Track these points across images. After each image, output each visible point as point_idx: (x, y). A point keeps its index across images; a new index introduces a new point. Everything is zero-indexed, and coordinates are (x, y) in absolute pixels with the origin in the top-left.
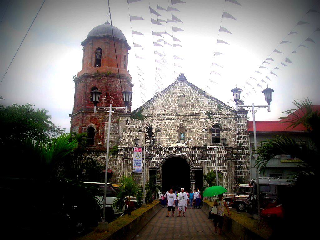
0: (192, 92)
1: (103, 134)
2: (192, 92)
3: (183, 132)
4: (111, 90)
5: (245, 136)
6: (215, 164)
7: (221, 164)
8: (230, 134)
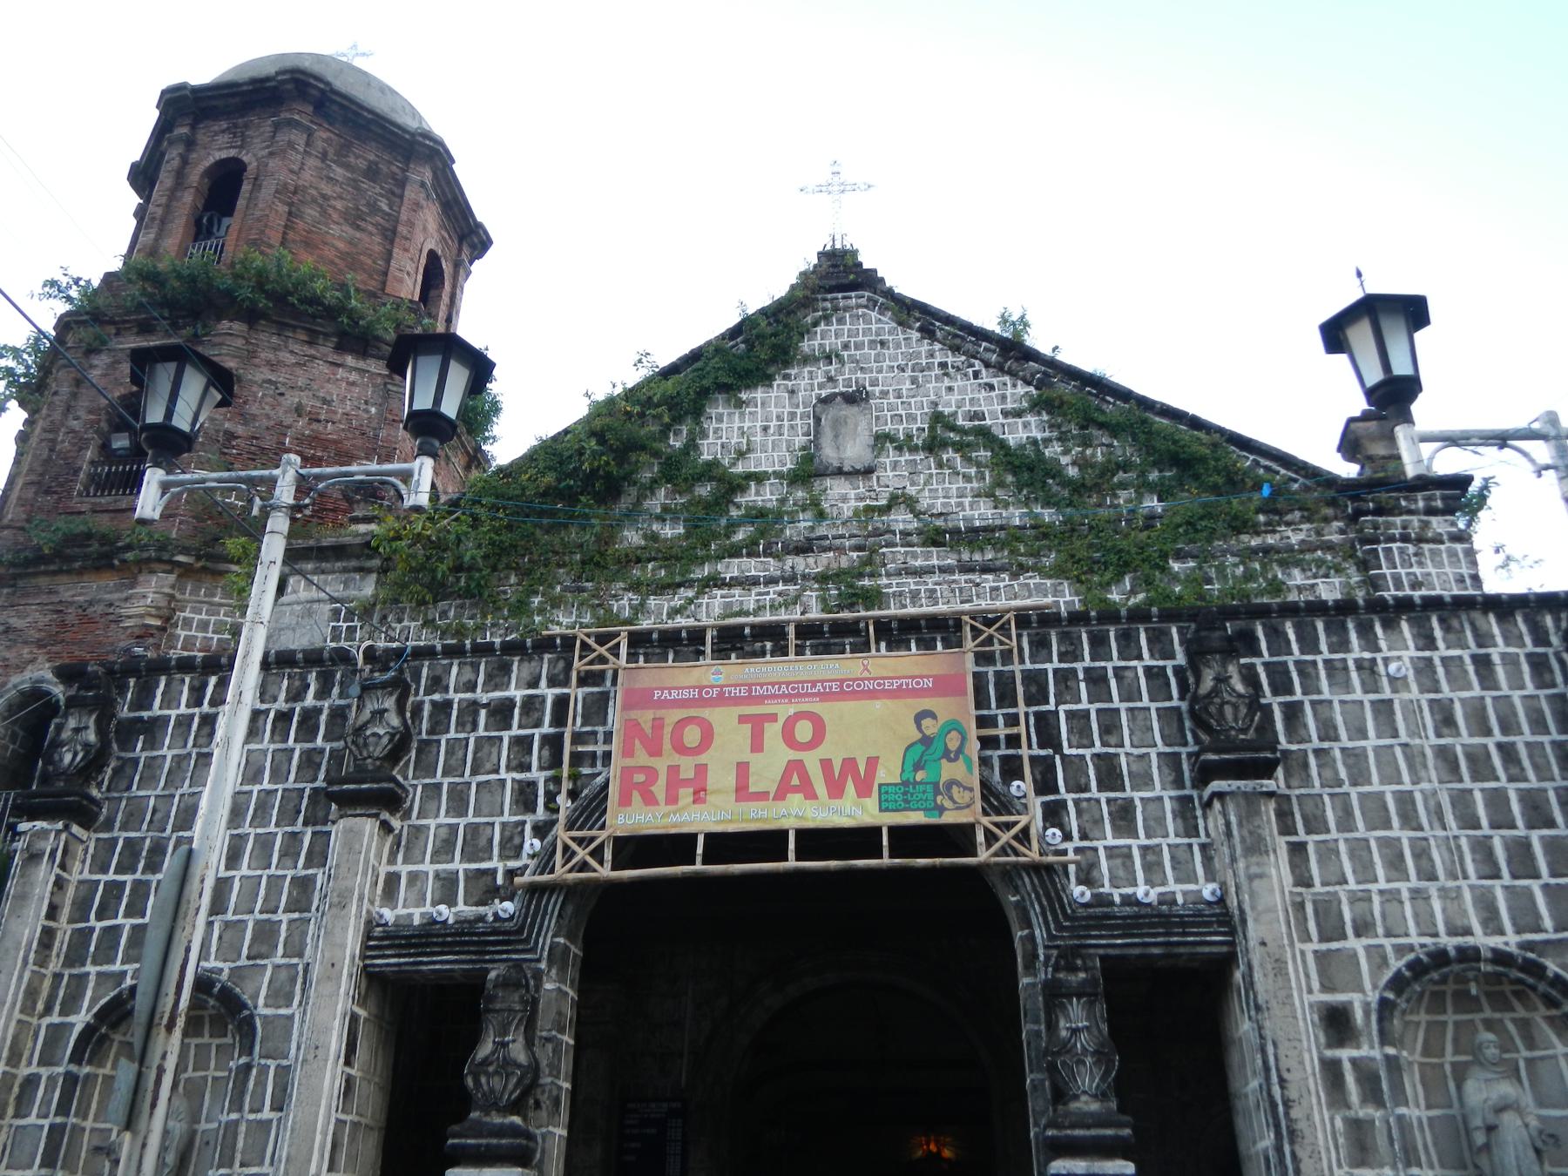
0: (929, 367)
4: (268, 417)
6: (1422, 853)
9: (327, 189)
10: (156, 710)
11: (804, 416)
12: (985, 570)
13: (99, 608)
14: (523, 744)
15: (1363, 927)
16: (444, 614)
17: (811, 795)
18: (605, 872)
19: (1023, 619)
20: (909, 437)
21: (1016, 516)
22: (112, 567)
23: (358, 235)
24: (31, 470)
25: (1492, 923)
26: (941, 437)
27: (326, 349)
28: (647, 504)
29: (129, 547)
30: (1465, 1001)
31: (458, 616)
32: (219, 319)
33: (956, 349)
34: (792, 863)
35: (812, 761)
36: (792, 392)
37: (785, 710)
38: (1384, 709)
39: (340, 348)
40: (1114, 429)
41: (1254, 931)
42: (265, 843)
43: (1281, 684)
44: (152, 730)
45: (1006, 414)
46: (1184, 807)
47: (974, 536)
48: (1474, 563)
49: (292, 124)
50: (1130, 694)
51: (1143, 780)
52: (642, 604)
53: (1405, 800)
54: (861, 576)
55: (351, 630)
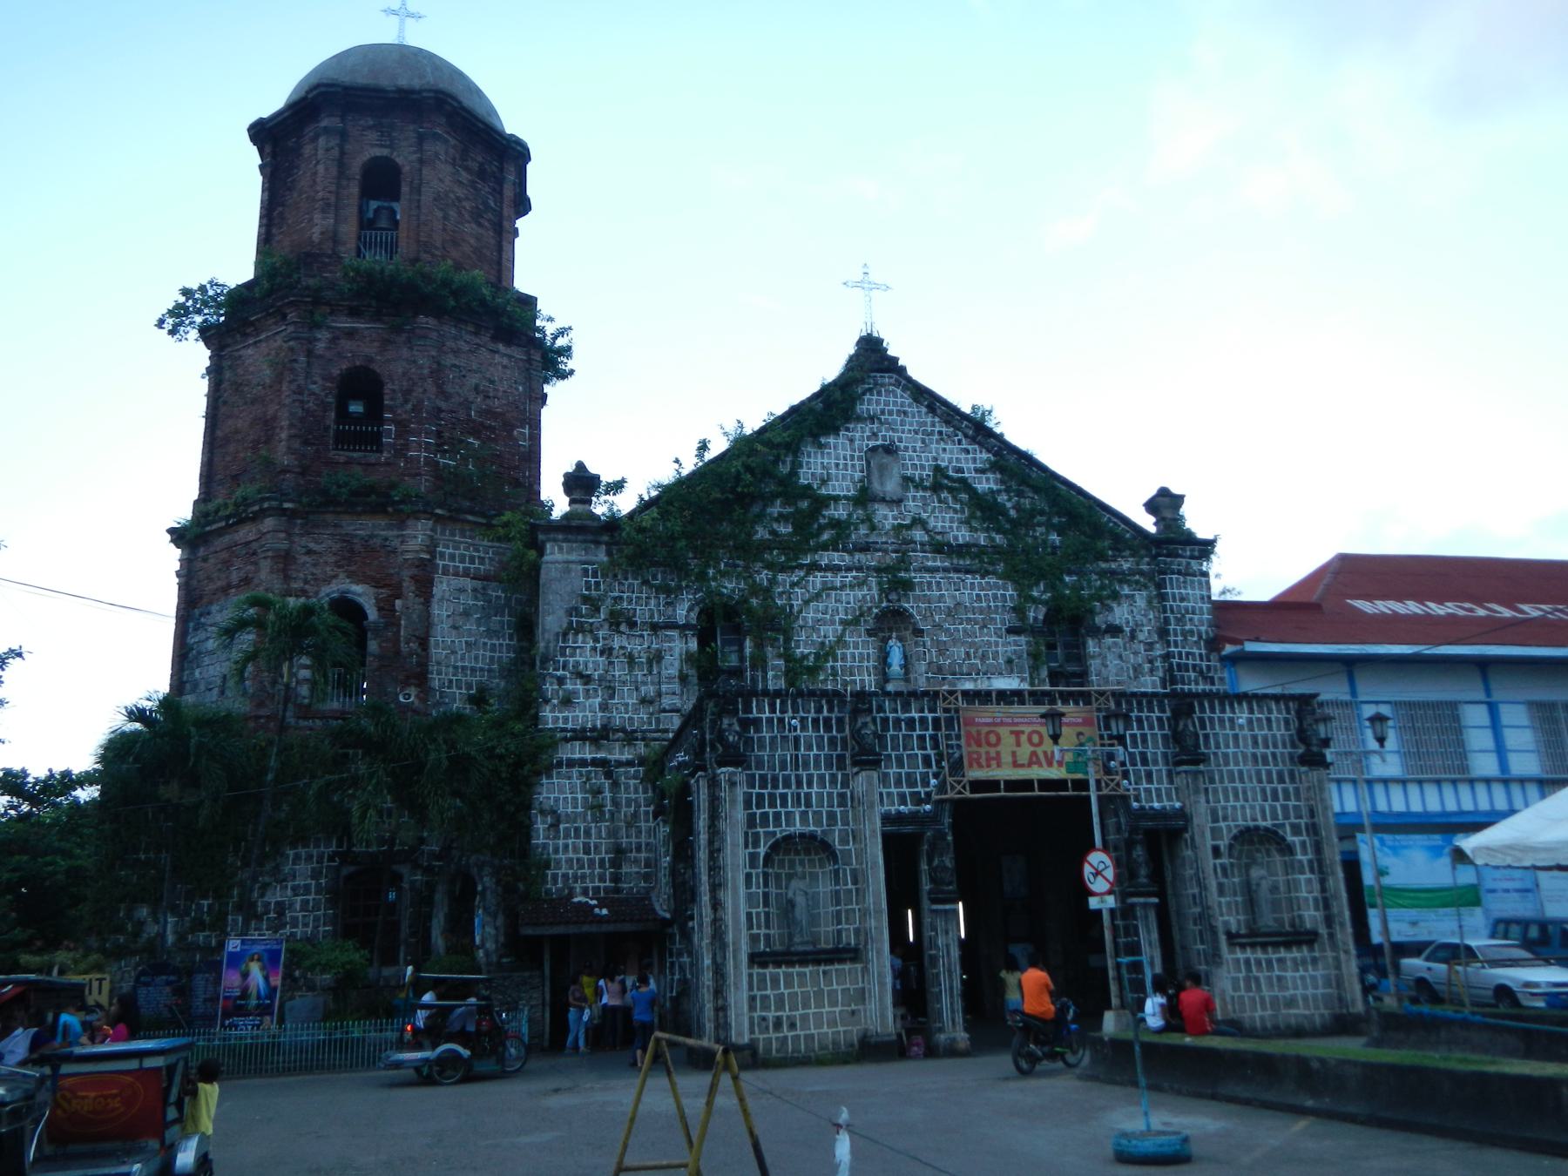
0: (932, 433)
1: (424, 643)
2: (932, 433)
3: (900, 639)
5: (1209, 667)
6: (1245, 792)
7: (1274, 792)
8: (1136, 653)
9: (460, 192)
10: (755, 714)
11: (860, 458)
12: (967, 572)
13: (378, 541)
14: (922, 738)
15: (1225, 819)
16: (655, 578)
17: (1040, 765)
18: (968, 794)
19: (1114, 693)
20: (922, 480)
21: (982, 539)
22: (386, 512)
23: (481, 231)
24: (291, 426)
25: (1264, 819)
26: (942, 482)
27: (485, 339)
28: (769, 510)
29: (402, 502)
30: (1251, 842)
31: (664, 579)
32: (416, 314)
33: (948, 423)
34: (1037, 793)
35: (1039, 751)
36: (852, 441)
37: (1028, 729)
38: (1236, 737)
39: (495, 339)
40: (1036, 490)
41: (1196, 821)
42: (821, 778)
43: (1203, 727)
44: (756, 722)
45: (977, 471)
46: (1170, 774)
47: (960, 550)
48: (1209, 588)
49: (436, 137)
50: (1151, 728)
51: (1155, 762)
52: (774, 577)
53: (1241, 772)
54: (899, 570)
55: (597, 584)
